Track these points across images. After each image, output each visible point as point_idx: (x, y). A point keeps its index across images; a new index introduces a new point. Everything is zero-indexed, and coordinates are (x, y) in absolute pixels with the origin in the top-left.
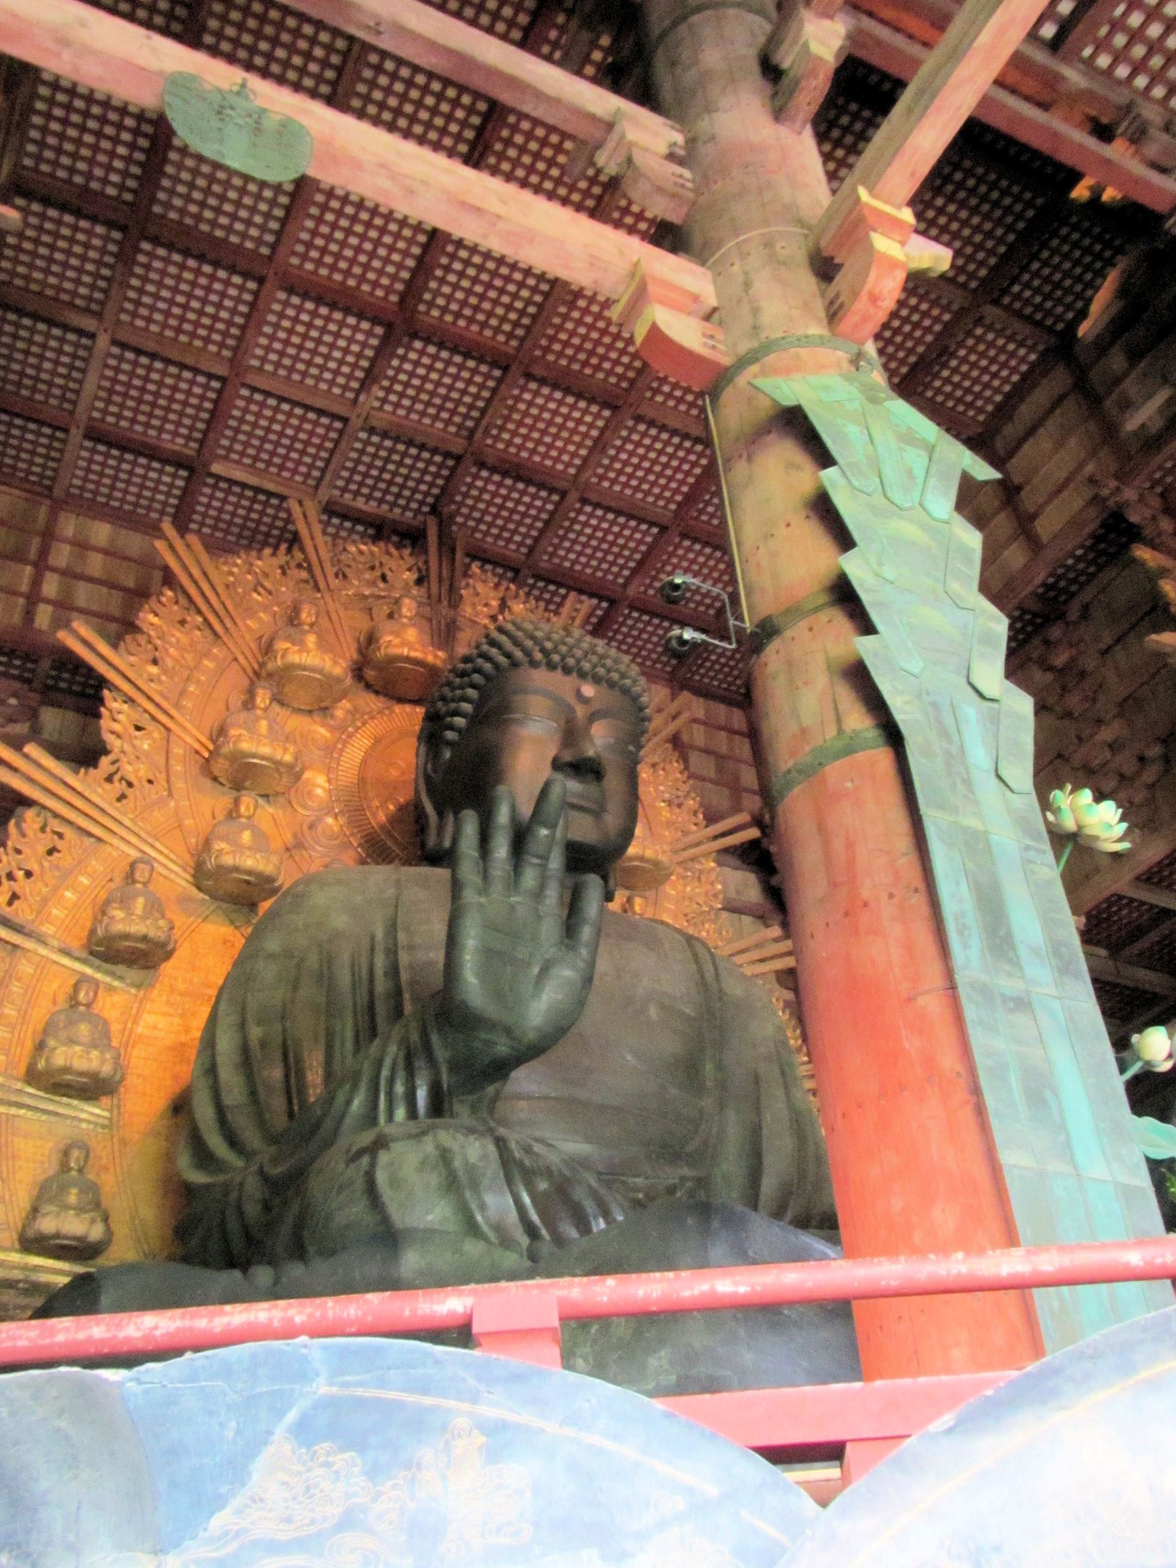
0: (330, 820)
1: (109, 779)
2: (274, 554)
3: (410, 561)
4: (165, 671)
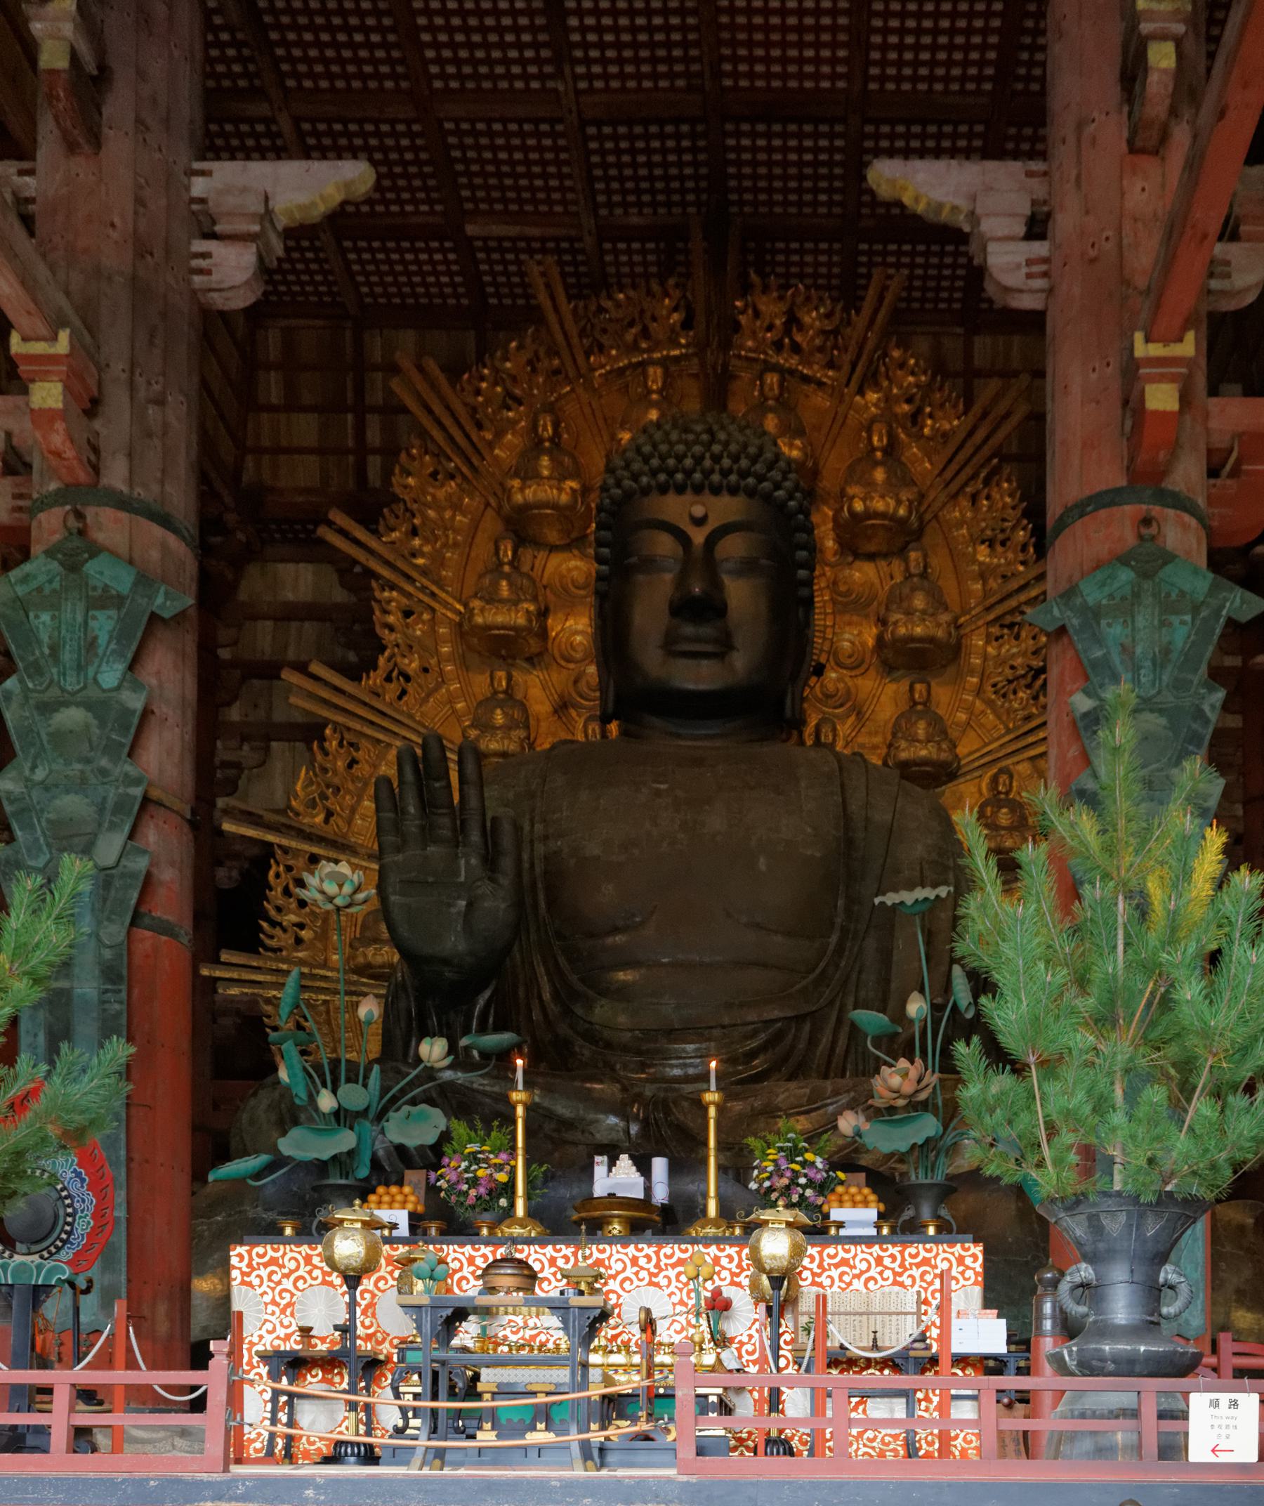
1: (388, 679)
4: (426, 540)
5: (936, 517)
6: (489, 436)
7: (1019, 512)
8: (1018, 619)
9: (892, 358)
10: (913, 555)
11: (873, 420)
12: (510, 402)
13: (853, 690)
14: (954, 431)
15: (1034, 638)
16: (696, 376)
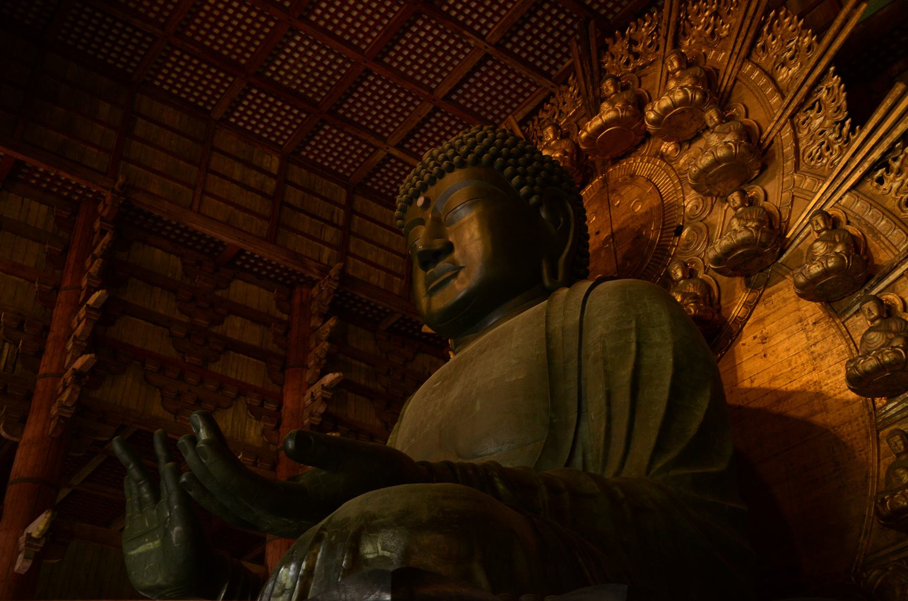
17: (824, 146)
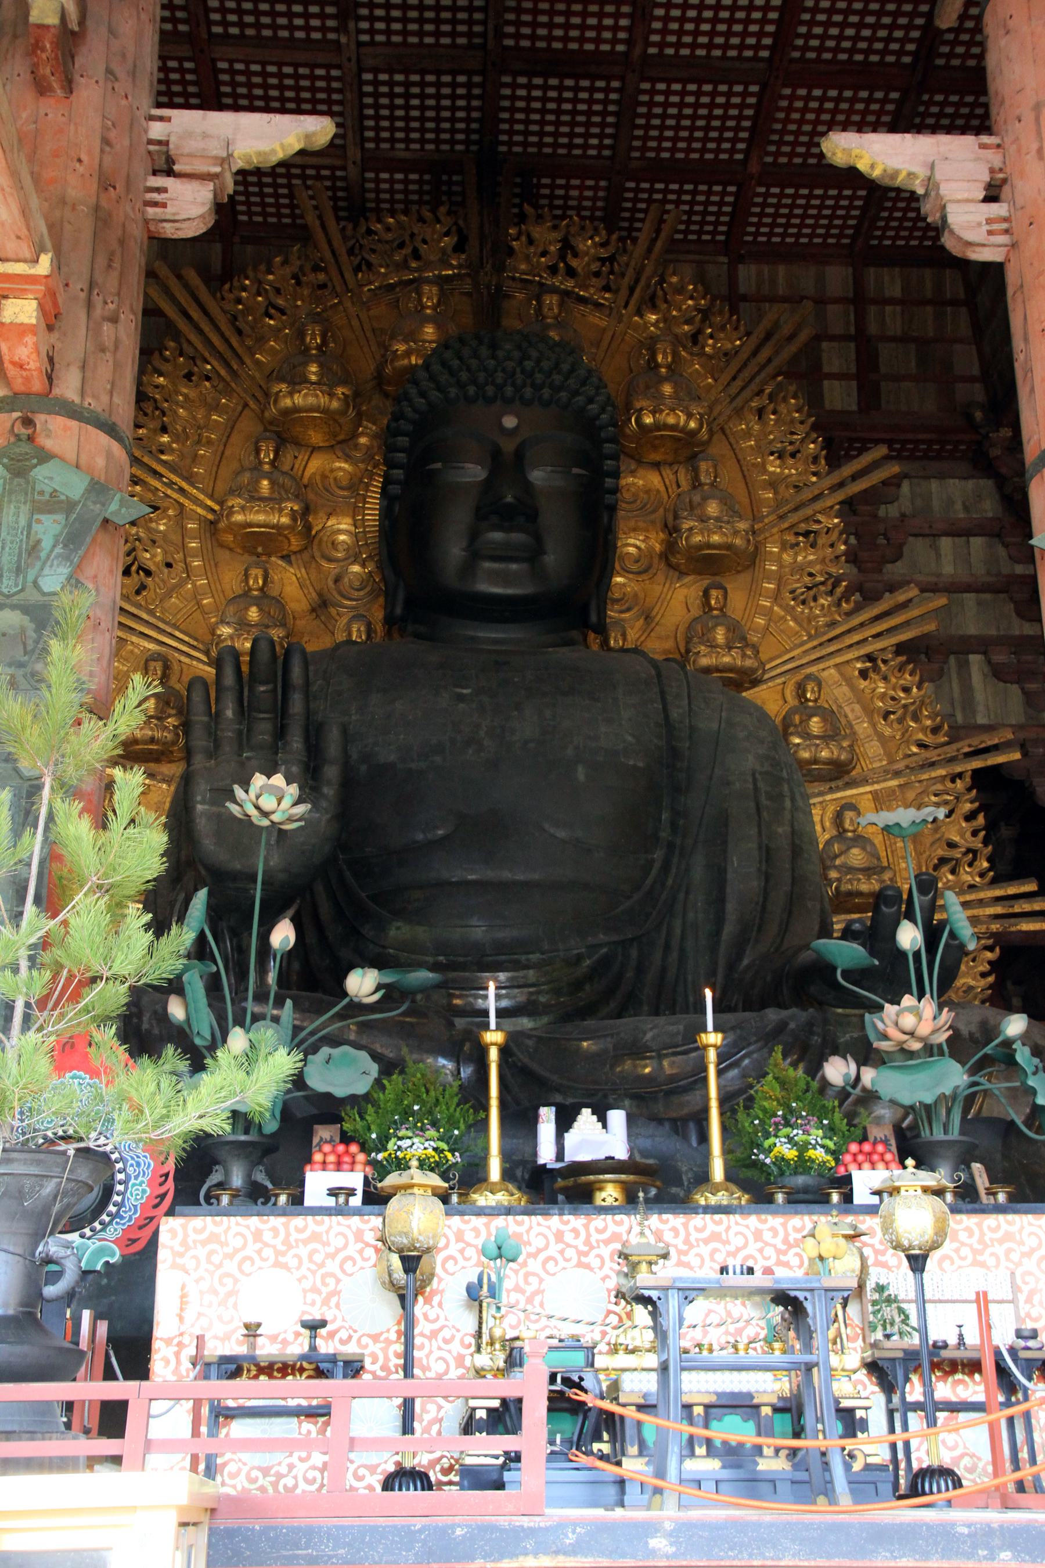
0: (356, 568)
2: (285, 262)
3: (448, 221)
4: (176, 438)
5: (722, 429)
6: (249, 342)
7: (807, 427)
8: (815, 527)
9: (670, 284)
10: (703, 466)
11: (653, 340)
12: (272, 311)
13: (641, 595)
14: (737, 351)
15: (832, 546)
16: (469, 294)
17: (812, 593)
